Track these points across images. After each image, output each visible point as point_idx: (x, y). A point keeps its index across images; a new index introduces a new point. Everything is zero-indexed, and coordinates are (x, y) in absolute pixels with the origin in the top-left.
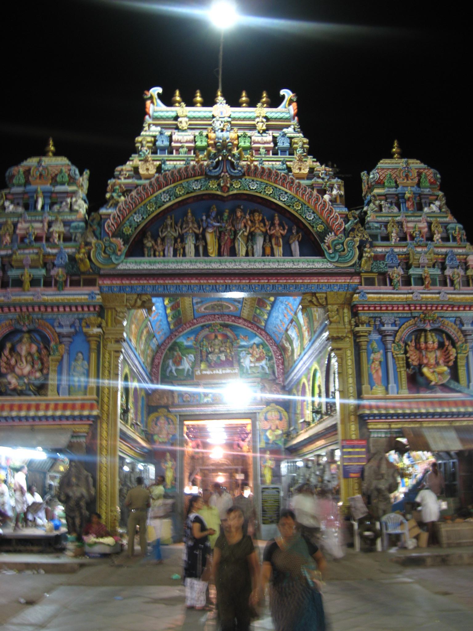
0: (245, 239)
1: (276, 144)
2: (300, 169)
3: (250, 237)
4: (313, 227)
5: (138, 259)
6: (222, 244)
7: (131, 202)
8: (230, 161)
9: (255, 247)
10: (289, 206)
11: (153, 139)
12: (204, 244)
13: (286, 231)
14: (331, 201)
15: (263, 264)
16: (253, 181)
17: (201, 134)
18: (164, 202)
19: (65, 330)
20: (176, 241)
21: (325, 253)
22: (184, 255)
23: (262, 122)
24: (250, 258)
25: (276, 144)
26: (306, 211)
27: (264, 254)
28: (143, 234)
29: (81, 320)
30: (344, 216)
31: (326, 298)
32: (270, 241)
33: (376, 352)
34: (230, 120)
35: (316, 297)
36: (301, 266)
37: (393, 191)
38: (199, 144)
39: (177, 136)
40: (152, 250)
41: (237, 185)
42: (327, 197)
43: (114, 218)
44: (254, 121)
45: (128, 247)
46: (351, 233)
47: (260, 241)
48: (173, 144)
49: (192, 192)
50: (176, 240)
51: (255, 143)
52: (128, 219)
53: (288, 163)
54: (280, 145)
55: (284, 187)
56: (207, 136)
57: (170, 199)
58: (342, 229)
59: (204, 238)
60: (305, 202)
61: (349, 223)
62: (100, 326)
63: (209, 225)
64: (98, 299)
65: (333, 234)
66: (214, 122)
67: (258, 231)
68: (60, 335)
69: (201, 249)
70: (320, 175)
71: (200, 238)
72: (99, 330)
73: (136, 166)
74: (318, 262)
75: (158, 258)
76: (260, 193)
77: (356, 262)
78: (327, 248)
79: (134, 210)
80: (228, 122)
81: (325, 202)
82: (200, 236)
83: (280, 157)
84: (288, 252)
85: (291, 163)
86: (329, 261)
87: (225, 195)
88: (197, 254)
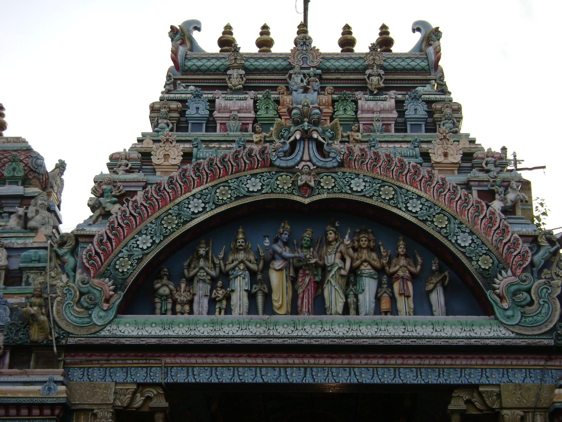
0: (343, 282)
1: (401, 113)
2: (446, 155)
3: (352, 279)
4: (470, 259)
5: (141, 318)
6: (300, 291)
7: (133, 212)
8: (316, 140)
9: (360, 297)
10: (425, 221)
11: (180, 105)
12: (266, 290)
13: (419, 267)
14: (505, 211)
15: (375, 328)
16: (357, 175)
17: (267, 98)
18: (193, 213)
20: (213, 286)
21: (495, 308)
22: (228, 311)
23: (379, 75)
24: (352, 317)
25: (401, 113)
26: (457, 230)
27: (378, 311)
28: (153, 271)
30: (531, 239)
31: (499, 395)
34: (319, 71)
35: (480, 394)
36: (448, 332)
38: (262, 113)
39: (222, 100)
40: (170, 300)
41: (327, 182)
42: (497, 205)
43: (101, 242)
44: (363, 73)
45: (122, 294)
46: (545, 271)
47: (369, 286)
48: (216, 114)
49: (245, 196)
50: (213, 281)
51: (363, 111)
52: (126, 245)
53: (424, 146)
54: (410, 113)
55: (417, 188)
56: (277, 102)
57: (204, 208)
58: (527, 263)
59: (267, 281)
60: (454, 214)
61: (541, 253)
63: (277, 256)
64: (61, 392)
65: (509, 272)
66: (291, 75)
69: (260, 299)
70: (484, 165)
73: (148, 150)
74: (480, 325)
75: (179, 316)
76: (371, 197)
77: (555, 325)
78: (498, 300)
79: (139, 228)
80: (315, 75)
81: (493, 213)
82: (259, 276)
83: (410, 135)
84: (422, 305)
85: (430, 146)
86: (502, 323)
87: (307, 201)
88: (252, 309)
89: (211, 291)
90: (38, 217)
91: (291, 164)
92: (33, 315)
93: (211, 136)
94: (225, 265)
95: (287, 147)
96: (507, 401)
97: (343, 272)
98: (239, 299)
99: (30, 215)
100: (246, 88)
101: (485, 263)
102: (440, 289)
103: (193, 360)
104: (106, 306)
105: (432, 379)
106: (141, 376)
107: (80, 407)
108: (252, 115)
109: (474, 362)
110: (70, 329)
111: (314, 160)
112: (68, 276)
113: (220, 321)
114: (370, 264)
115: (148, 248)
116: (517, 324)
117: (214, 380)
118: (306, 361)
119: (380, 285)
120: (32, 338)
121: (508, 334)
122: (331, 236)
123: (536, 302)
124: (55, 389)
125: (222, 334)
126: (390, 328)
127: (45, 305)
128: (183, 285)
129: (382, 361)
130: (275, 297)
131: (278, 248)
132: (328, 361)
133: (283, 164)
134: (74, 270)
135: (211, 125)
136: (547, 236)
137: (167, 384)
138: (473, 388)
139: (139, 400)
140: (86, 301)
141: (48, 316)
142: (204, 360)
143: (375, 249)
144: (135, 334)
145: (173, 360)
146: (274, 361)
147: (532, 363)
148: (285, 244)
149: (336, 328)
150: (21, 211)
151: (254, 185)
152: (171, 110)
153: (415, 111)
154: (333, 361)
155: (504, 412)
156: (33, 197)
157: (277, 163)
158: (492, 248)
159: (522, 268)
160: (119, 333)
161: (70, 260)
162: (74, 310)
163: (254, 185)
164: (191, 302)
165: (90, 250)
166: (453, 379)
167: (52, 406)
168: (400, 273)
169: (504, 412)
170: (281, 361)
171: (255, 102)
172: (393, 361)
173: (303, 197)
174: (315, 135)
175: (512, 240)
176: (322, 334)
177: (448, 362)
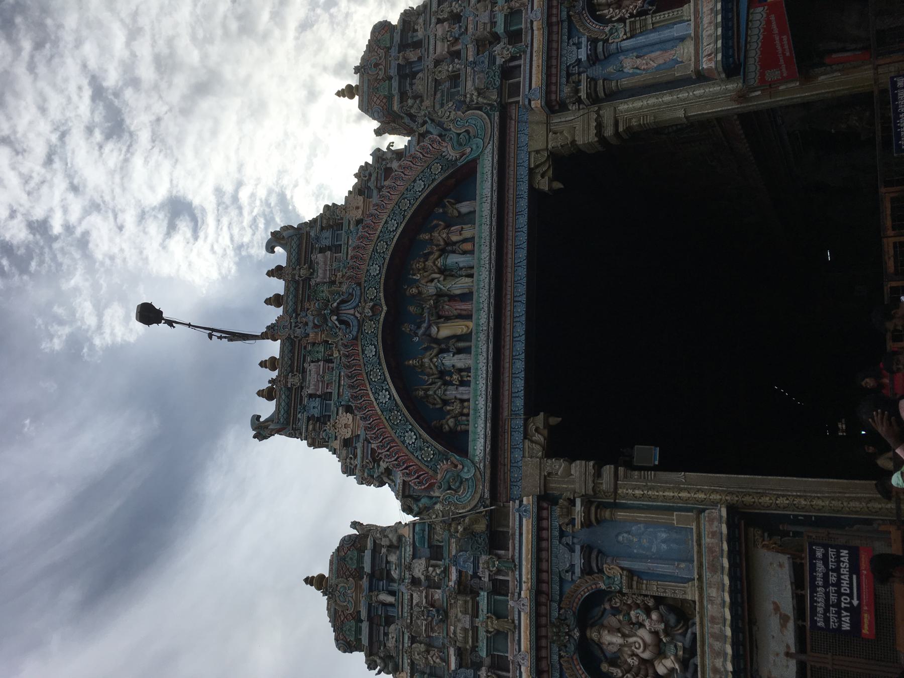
2: (357, 208)
3: (447, 273)
4: (433, 180)
6: (455, 312)
9: (461, 265)
10: (404, 216)
11: (311, 422)
19: (578, 560)
20: (450, 383)
22: (468, 370)
24: (475, 271)
27: (472, 252)
28: (436, 433)
29: (562, 534)
31: (537, 152)
32: (455, 243)
33: (622, 66)
35: (537, 167)
37: (395, 84)
41: (371, 293)
52: (412, 453)
54: (328, 243)
62: (572, 502)
63: (428, 333)
64: (528, 501)
67: (440, 263)
68: (587, 571)
69: (461, 345)
71: (443, 346)
72: (578, 502)
76: (384, 259)
82: (443, 346)
84: (468, 218)
87: (385, 308)
89: (454, 385)
90: (390, 536)
91: (355, 323)
92: (464, 529)
93: (335, 396)
94: (433, 374)
95: (343, 327)
96: (540, 145)
97: (442, 279)
98: (459, 361)
99: (388, 543)
100: (304, 371)
101: (437, 168)
102: (458, 206)
103: (506, 393)
104: (460, 467)
105: (524, 203)
106: (518, 437)
107: (542, 488)
108: (321, 363)
109: (512, 173)
110: (478, 496)
111: (354, 304)
112: (435, 503)
113: (477, 371)
114: (437, 259)
115: (415, 434)
117: (522, 375)
118: (509, 301)
119: (454, 252)
120: (484, 529)
121: (490, 146)
122: (414, 291)
124: (526, 506)
125: (485, 368)
126: (483, 235)
127: (458, 519)
128: (448, 408)
129: (510, 242)
130: (459, 332)
131: (421, 332)
132: (509, 284)
133: (355, 329)
134: (431, 498)
135: (326, 396)
137: (525, 414)
138: (531, 172)
139: (538, 437)
140: (455, 483)
141: (465, 516)
142: (507, 383)
143: (426, 257)
144: (482, 441)
145: (506, 410)
146: (508, 327)
147: (513, 130)
148: (419, 327)
149: (482, 277)
150: (384, 550)
151: (370, 351)
152: (314, 429)
153: (326, 238)
154: (509, 280)
155: (550, 147)
156: (374, 541)
157: (355, 333)
158: (427, 165)
160: (482, 455)
161: (424, 501)
162: (463, 493)
163: (370, 351)
164: (462, 401)
165: (415, 483)
166: (524, 187)
167: (540, 509)
168: (444, 236)
169: (550, 147)
170: (508, 321)
171: (313, 362)
172: (510, 234)
173: (381, 312)
174: (335, 304)
176: (487, 287)
177: (511, 191)
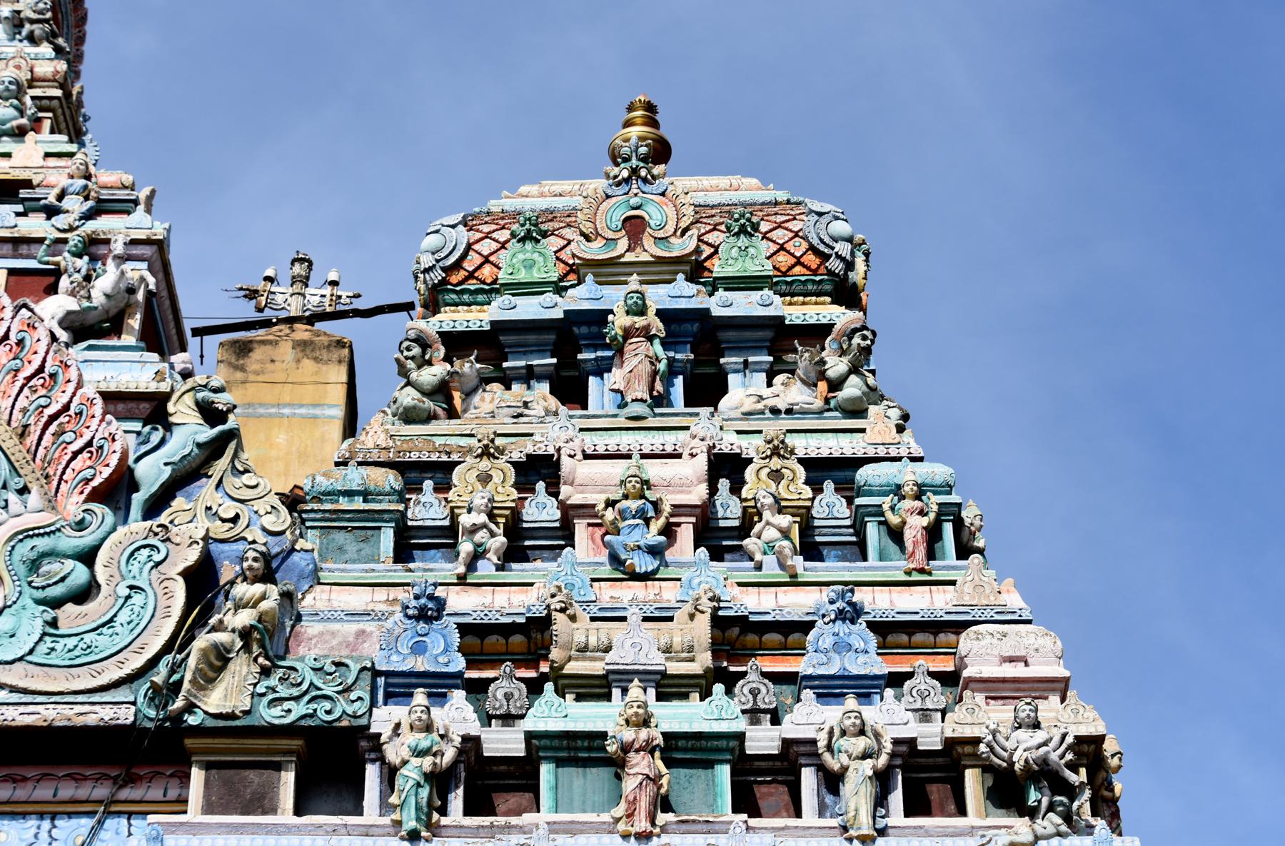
30: (145, 407)
42: (54, 307)
116: (21, 659)
123: (105, 590)
136: (200, 395)
159: (88, 489)
175: (73, 406)
